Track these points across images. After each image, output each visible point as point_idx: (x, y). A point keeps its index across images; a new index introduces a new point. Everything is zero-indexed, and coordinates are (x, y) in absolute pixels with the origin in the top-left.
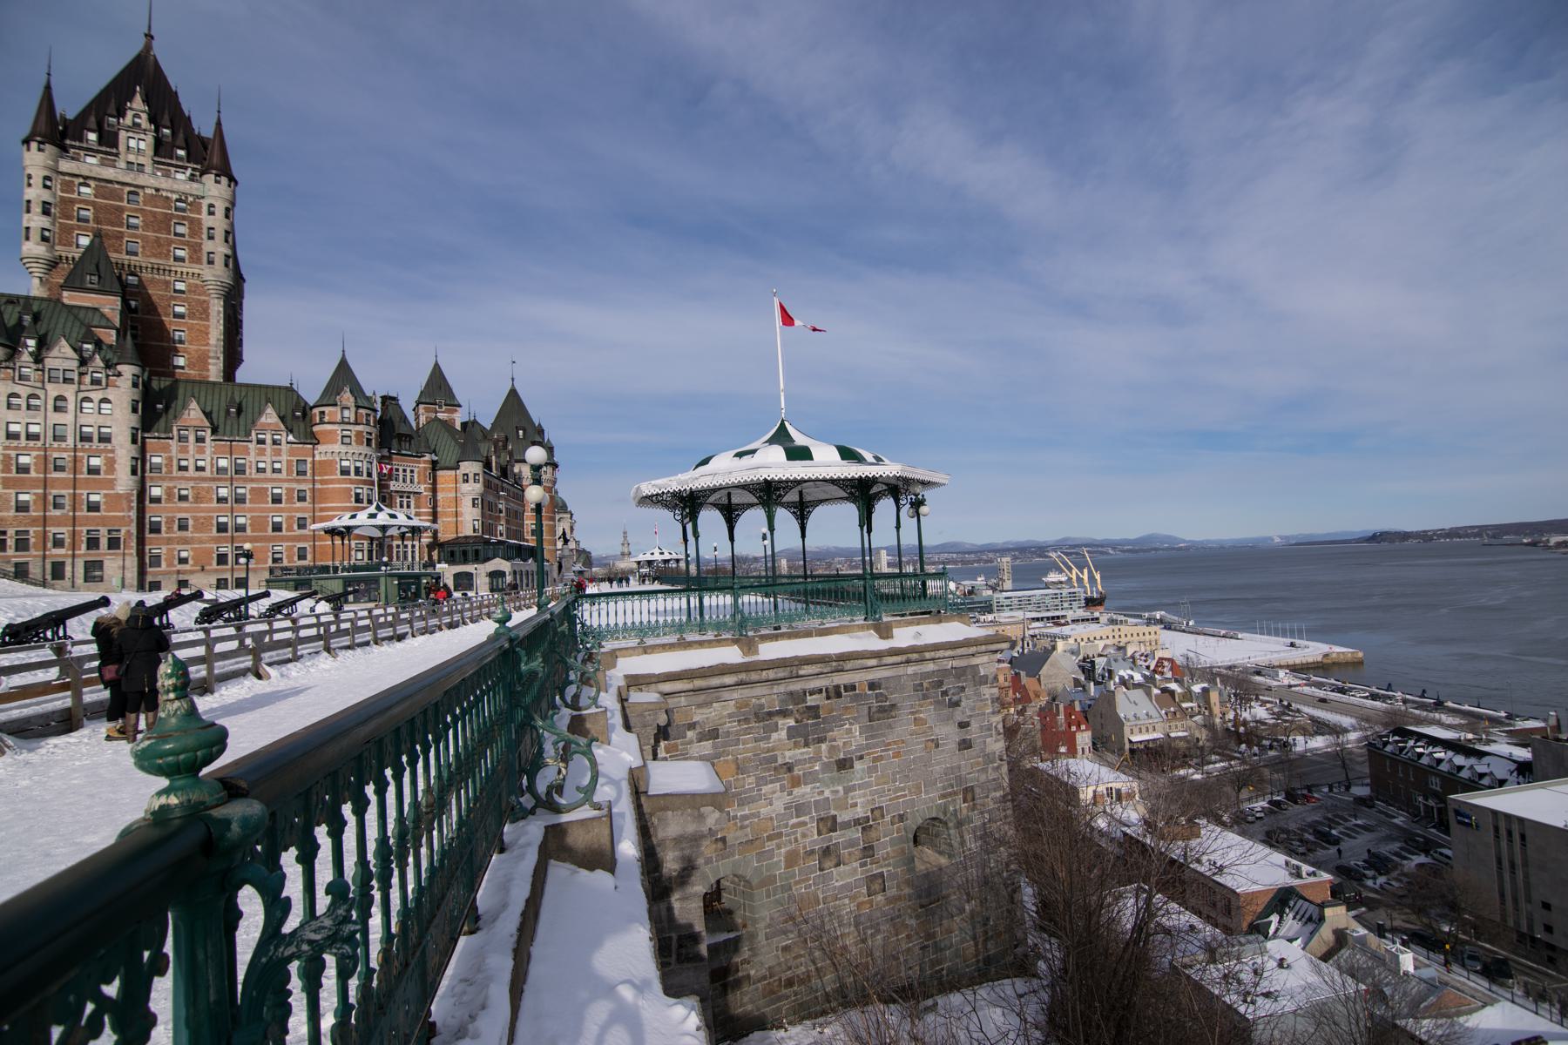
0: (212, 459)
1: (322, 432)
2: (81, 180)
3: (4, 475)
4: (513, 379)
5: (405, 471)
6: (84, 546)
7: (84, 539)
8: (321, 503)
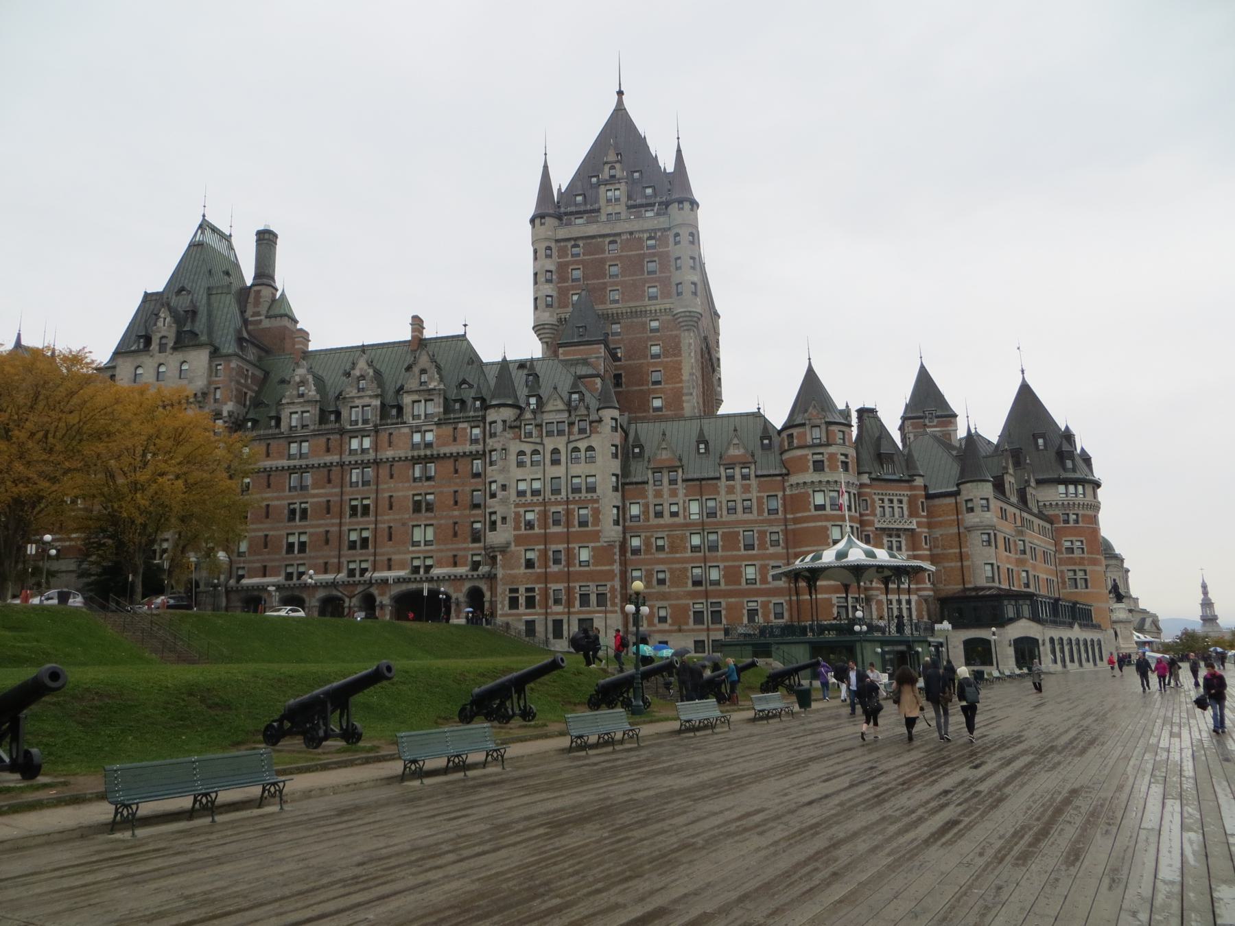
0: (684, 502)
1: (792, 459)
2: (573, 243)
3: (516, 532)
4: (1023, 372)
5: (891, 501)
6: (577, 603)
7: (577, 596)
8: (795, 548)
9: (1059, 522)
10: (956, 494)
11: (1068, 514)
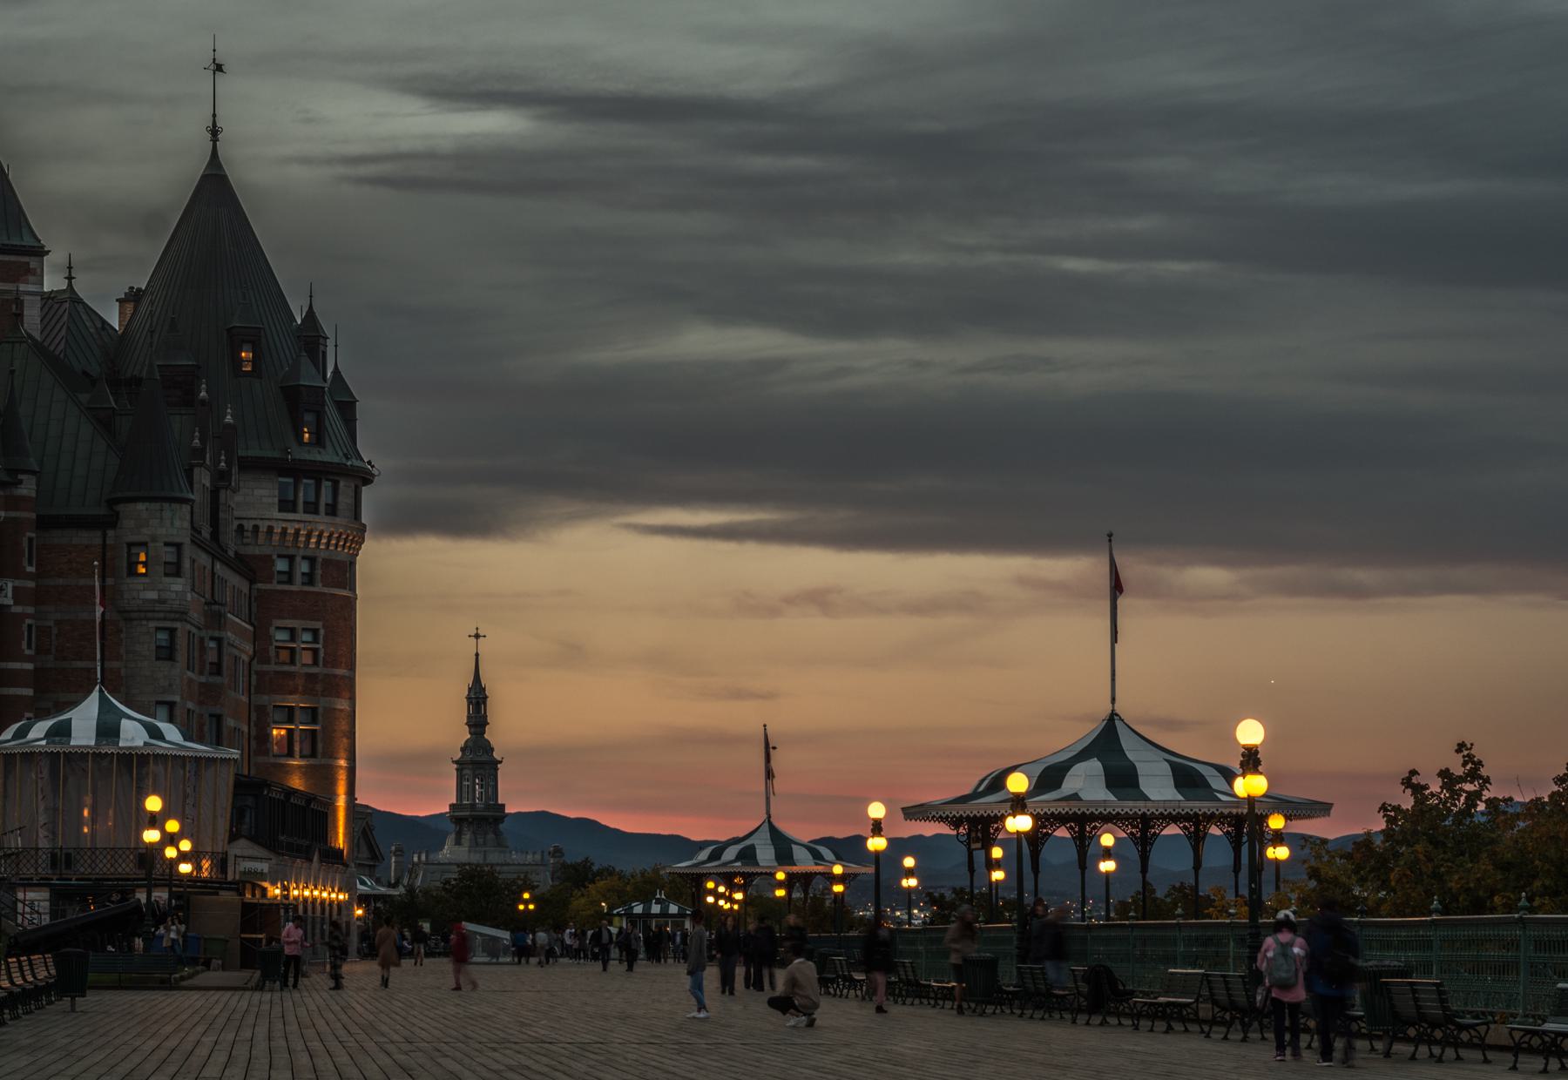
4: (214, 132)
9: (269, 580)
10: (109, 522)
11: (291, 559)
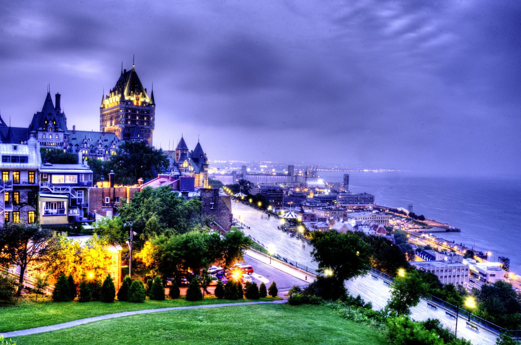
1: (181, 169)
